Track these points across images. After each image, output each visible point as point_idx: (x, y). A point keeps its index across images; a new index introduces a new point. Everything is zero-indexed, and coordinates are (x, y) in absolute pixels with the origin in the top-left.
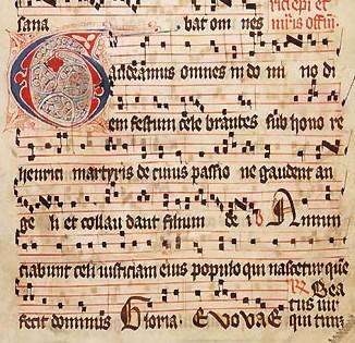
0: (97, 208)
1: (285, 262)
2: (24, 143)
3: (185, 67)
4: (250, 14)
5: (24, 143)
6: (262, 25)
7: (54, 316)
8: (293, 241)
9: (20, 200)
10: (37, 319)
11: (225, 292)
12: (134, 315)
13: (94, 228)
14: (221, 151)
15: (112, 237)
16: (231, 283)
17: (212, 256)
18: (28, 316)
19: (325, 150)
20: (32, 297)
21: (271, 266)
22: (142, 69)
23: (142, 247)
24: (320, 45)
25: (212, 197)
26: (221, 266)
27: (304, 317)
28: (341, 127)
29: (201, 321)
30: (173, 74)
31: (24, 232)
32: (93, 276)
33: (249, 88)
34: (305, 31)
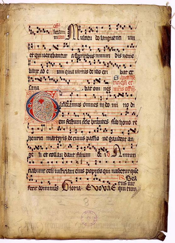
0: (55, 150)
1: (117, 169)
2: (30, 128)
3: (85, 103)
4: (106, 86)
5: (30, 128)
6: (110, 89)
7: (39, 186)
8: (120, 162)
9: (29, 147)
10: (34, 187)
11: (97, 179)
12: (66, 186)
13: (53, 157)
14: (96, 131)
15: (59, 160)
16: (99, 175)
17: (93, 166)
18: (31, 186)
19: (131, 132)
20: (32, 180)
21: (112, 170)
22: (70, 103)
23: (69, 163)
24: (129, 96)
25: (93, 147)
26: (96, 170)
27: (123, 188)
28: (136, 124)
29: (89, 188)
30: (81, 105)
31: (30, 158)
32: (53, 173)
33: (106, 110)
34: (124, 92)
